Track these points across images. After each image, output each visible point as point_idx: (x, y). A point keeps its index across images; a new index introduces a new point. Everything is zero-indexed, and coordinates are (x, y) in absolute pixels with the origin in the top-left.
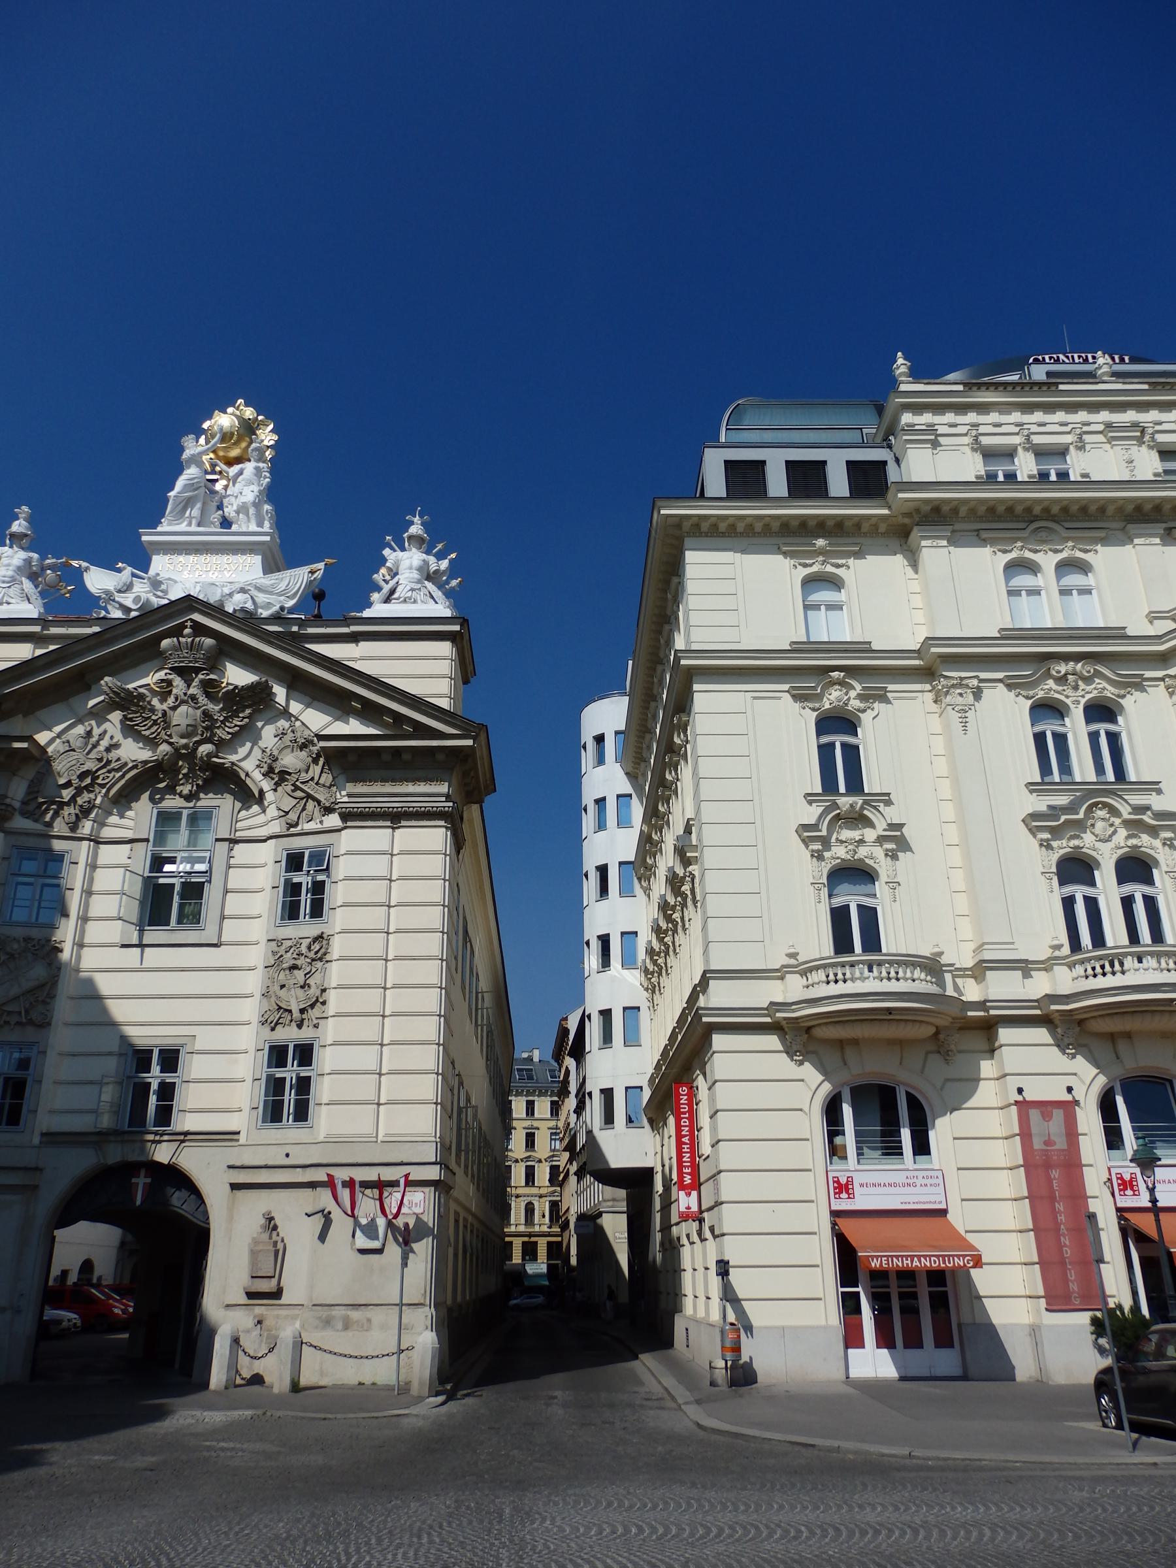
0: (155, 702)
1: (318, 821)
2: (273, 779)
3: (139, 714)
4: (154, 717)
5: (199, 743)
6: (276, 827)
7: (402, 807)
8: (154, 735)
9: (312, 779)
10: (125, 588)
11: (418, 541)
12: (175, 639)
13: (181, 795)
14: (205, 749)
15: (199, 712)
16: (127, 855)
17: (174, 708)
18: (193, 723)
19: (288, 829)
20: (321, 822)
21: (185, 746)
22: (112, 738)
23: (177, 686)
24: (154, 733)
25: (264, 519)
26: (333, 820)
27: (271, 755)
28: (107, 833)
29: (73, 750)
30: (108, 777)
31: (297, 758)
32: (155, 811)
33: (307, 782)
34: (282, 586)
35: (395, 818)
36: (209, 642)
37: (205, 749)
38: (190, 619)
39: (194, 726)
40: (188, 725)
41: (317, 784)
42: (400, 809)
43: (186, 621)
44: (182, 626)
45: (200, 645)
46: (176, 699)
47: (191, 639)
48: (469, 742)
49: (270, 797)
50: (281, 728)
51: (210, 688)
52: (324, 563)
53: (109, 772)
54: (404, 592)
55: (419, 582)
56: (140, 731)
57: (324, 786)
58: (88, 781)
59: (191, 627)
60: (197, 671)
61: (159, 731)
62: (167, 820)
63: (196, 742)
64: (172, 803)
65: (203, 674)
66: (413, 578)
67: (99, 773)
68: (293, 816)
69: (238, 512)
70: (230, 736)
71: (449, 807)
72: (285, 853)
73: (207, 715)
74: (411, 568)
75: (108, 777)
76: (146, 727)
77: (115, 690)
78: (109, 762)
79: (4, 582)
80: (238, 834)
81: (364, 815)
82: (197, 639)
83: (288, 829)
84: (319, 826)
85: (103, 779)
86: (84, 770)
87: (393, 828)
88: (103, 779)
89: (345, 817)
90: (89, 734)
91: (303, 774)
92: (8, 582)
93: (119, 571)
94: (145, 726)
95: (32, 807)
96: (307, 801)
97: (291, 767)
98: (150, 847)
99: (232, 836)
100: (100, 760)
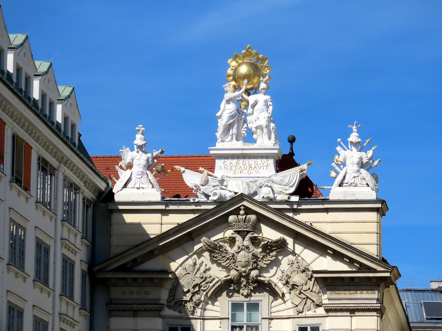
0: (228, 248)
1: (313, 310)
2: (289, 287)
3: (219, 255)
4: (228, 256)
5: (251, 270)
6: (292, 313)
7: (355, 307)
8: (228, 265)
9: (309, 289)
10: (205, 183)
11: (355, 144)
12: (236, 216)
13: (242, 295)
14: (254, 273)
15: (250, 254)
16: (219, 326)
17: (238, 253)
18: (248, 260)
19: (298, 314)
20: (315, 312)
21: (245, 272)
22: (206, 265)
23: (238, 241)
24: (228, 264)
25: (271, 132)
26: (321, 311)
27: (287, 275)
28: (207, 314)
29: (189, 273)
30: (206, 286)
31: (301, 277)
32: (230, 303)
33: (307, 290)
34: (286, 181)
35: (352, 311)
36: (253, 217)
37: (254, 273)
38: (243, 205)
39: (249, 262)
40: (245, 261)
41: (311, 291)
42: (354, 308)
43: (241, 206)
44: (239, 209)
45: (249, 220)
46: (239, 248)
47: (245, 216)
48: (388, 275)
49: (287, 296)
50: (291, 261)
51: (255, 241)
52: (307, 164)
53: (207, 283)
54: (350, 179)
55: (358, 171)
56: (221, 263)
57: (315, 292)
58: (197, 289)
59: (244, 209)
60: (248, 232)
61: (230, 263)
62: (236, 307)
63: (250, 270)
64: (238, 298)
65: (251, 234)
66: (355, 170)
67: (202, 284)
68: (300, 308)
69: (257, 128)
70: (266, 265)
71: (379, 306)
72: (297, 327)
73: (255, 256)
74: (353, 164)
75: (206, 286)
76: (224, 261)
77: (208, 244)
78: (206, 278)
79: (138, 175)
80: (273, 314)
81: (337, 310)
82: (248, 216)
83: (298, 314)
84: (314, 313)
85: (204, 287)
86: (195, 283)
87: (351, 316)
88: (204, 287)
89: (327, 311)
90: (195, 264)
91: (304, 286)
92: (141, 175)
93: (201, 172)
94: (223, 260)
95: (172, 303)
96: (307, 300)
97: (297, 282)
98: (230, 322)
99: (270, 317)
100: (202, 278)
